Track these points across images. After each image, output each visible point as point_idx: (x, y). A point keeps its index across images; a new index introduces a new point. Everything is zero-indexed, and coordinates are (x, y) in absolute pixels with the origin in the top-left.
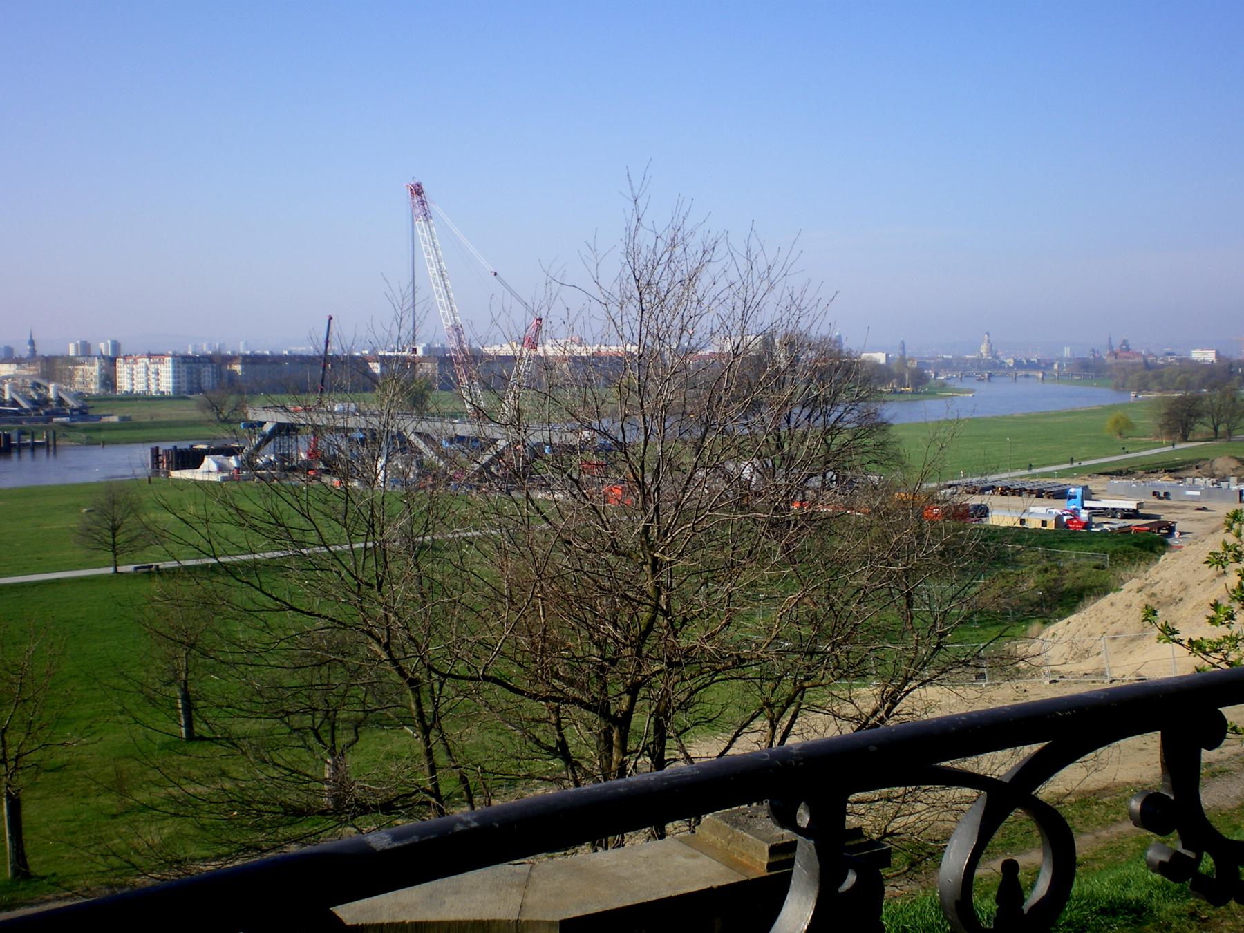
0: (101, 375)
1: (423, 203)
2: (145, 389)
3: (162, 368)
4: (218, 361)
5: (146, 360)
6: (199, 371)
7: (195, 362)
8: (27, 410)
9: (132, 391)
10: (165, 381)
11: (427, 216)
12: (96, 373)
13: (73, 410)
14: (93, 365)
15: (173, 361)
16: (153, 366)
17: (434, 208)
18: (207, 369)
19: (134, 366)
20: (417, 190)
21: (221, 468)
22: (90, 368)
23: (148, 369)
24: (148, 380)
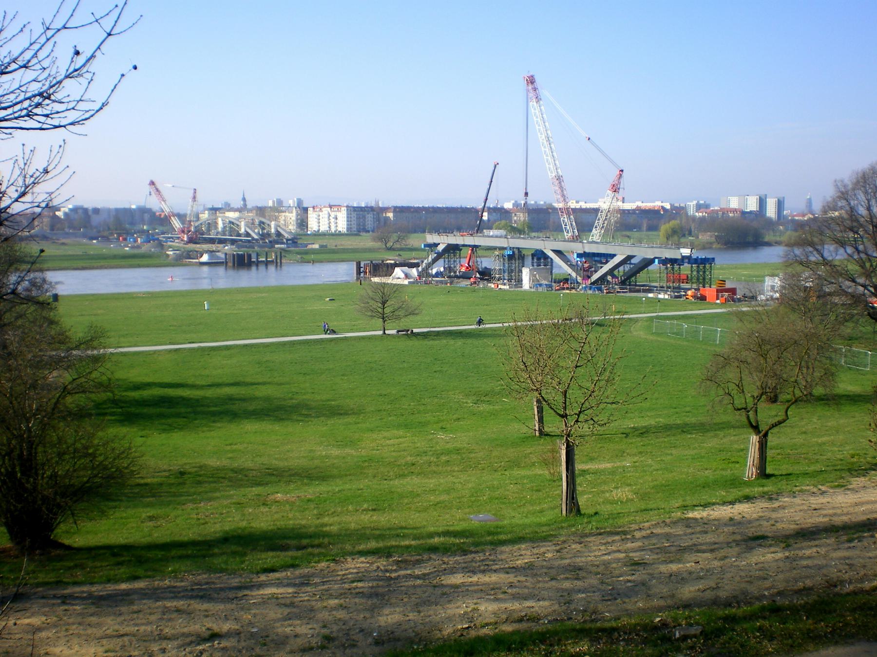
0: (297, 219)
1: (535, 89)
2: (328, 229)
3: (339, 215)
4: (377, 211)
5: (329, 209)
6: (364, 217)
7: (362, 211)
8: (257, 240)
9: (319, 230)
10: (342, 225)
11: (538, 99)
12: (294, 218)
13: (287, 240)
14: (292, 213)
15: (347, 210)
16: (333, 213)
17: (544, 93)
18: (369, 215)
19: (320, 213)
20: (531, 81)
21: (407, 276)
22: (291, 215)
23: (330, 215)
24: (330, 223)
